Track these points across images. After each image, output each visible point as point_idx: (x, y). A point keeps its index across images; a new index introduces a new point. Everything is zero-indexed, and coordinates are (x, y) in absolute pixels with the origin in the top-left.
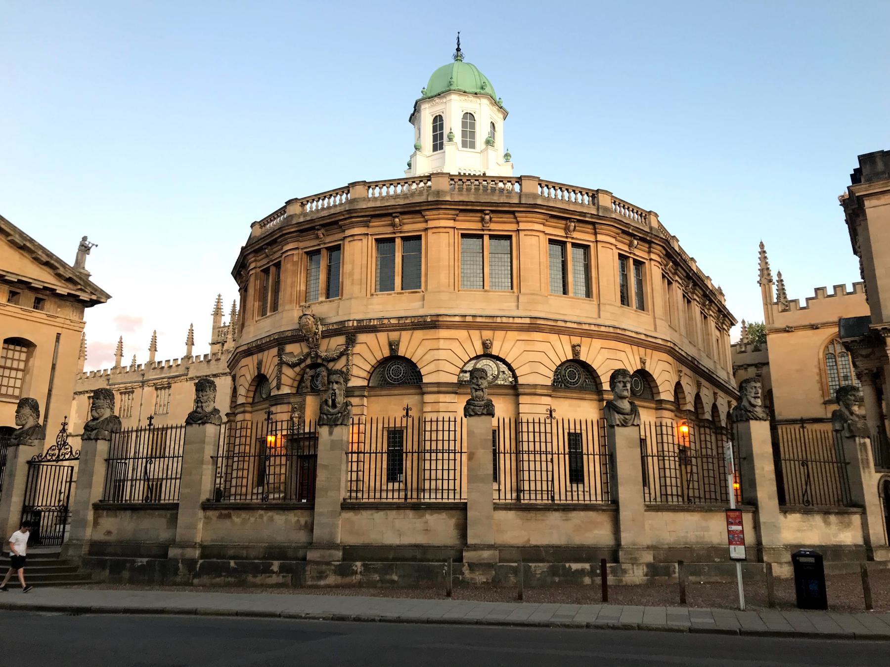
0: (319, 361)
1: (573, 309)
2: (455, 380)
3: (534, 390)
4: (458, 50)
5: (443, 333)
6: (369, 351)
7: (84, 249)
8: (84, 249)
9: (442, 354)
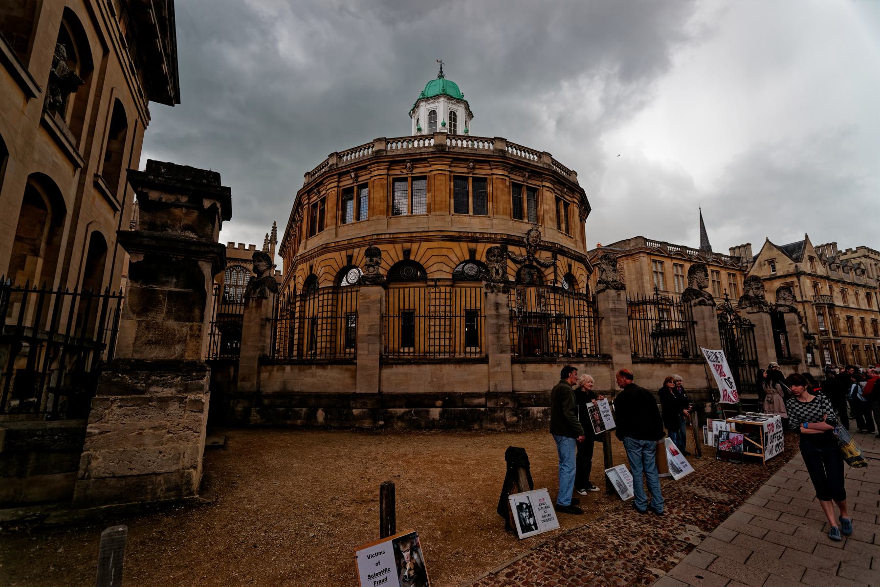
0: (535, 264)
4: (441, 72)
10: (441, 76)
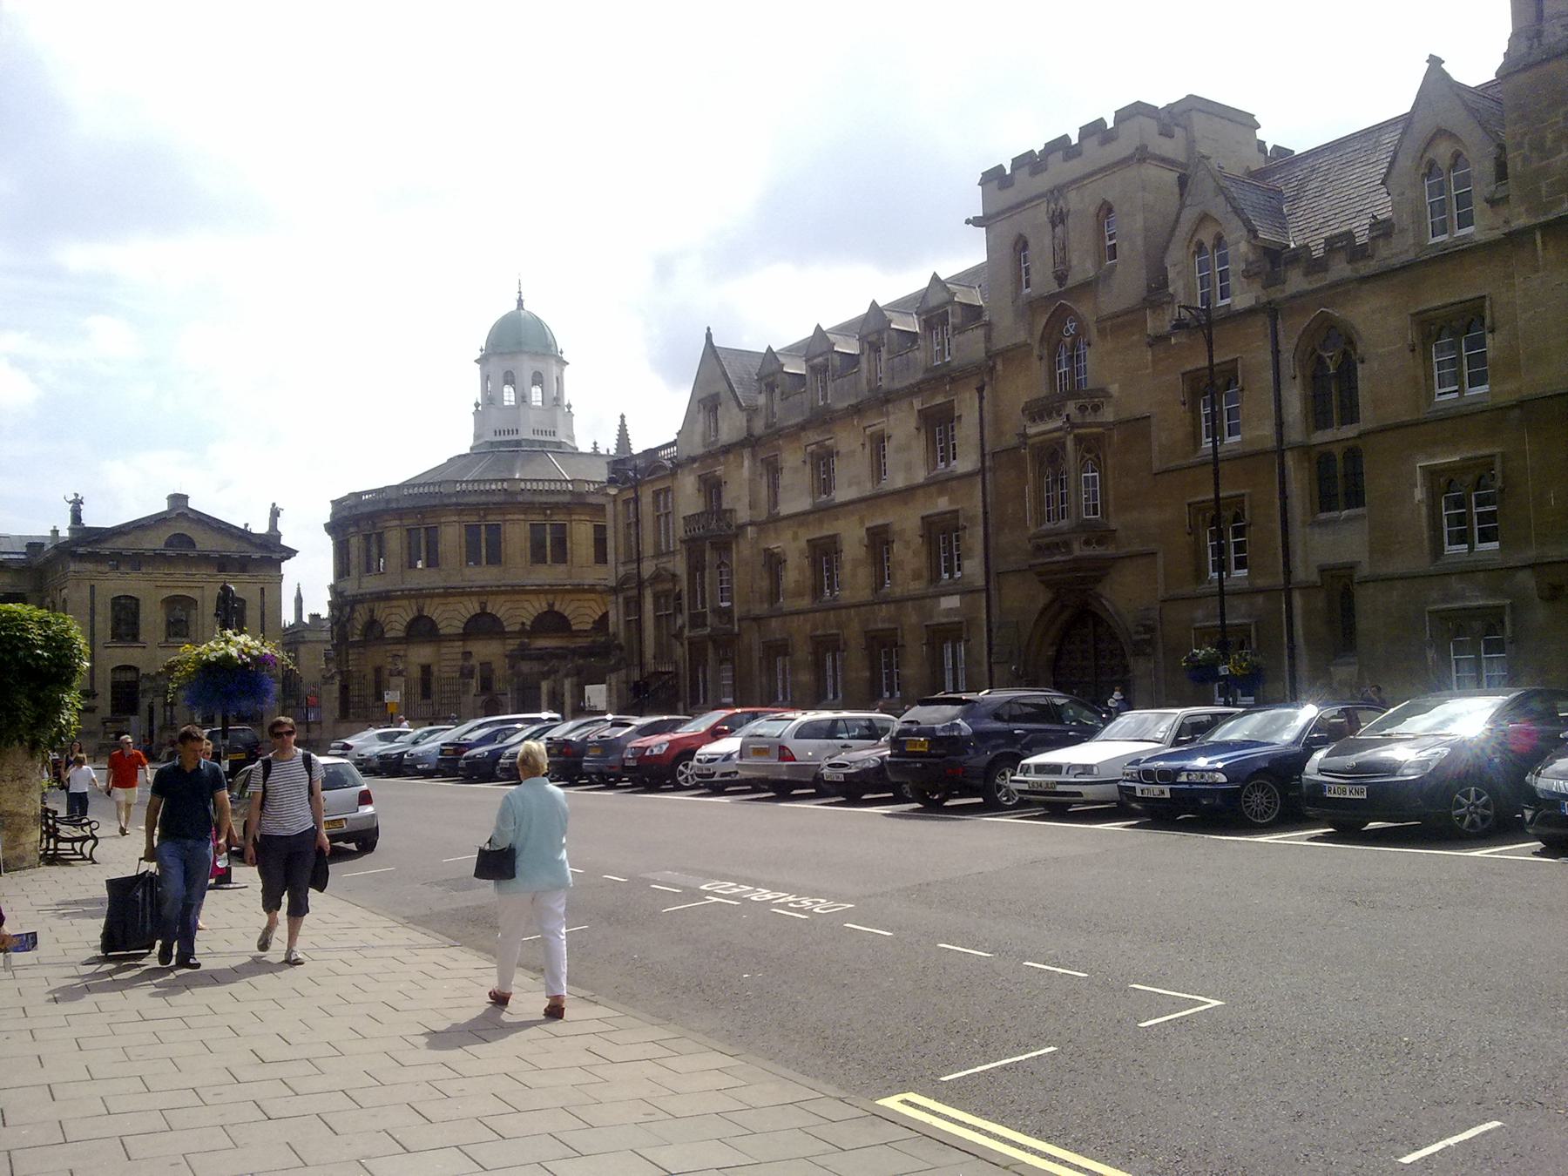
1: (484, 575)
2: (402, 634)
3: (450, 638)
5: (395, 603)
6: (361, 615)
7: (275, 513)
8: (275, 513)
9: (393, 618)
10: (520, 302)
